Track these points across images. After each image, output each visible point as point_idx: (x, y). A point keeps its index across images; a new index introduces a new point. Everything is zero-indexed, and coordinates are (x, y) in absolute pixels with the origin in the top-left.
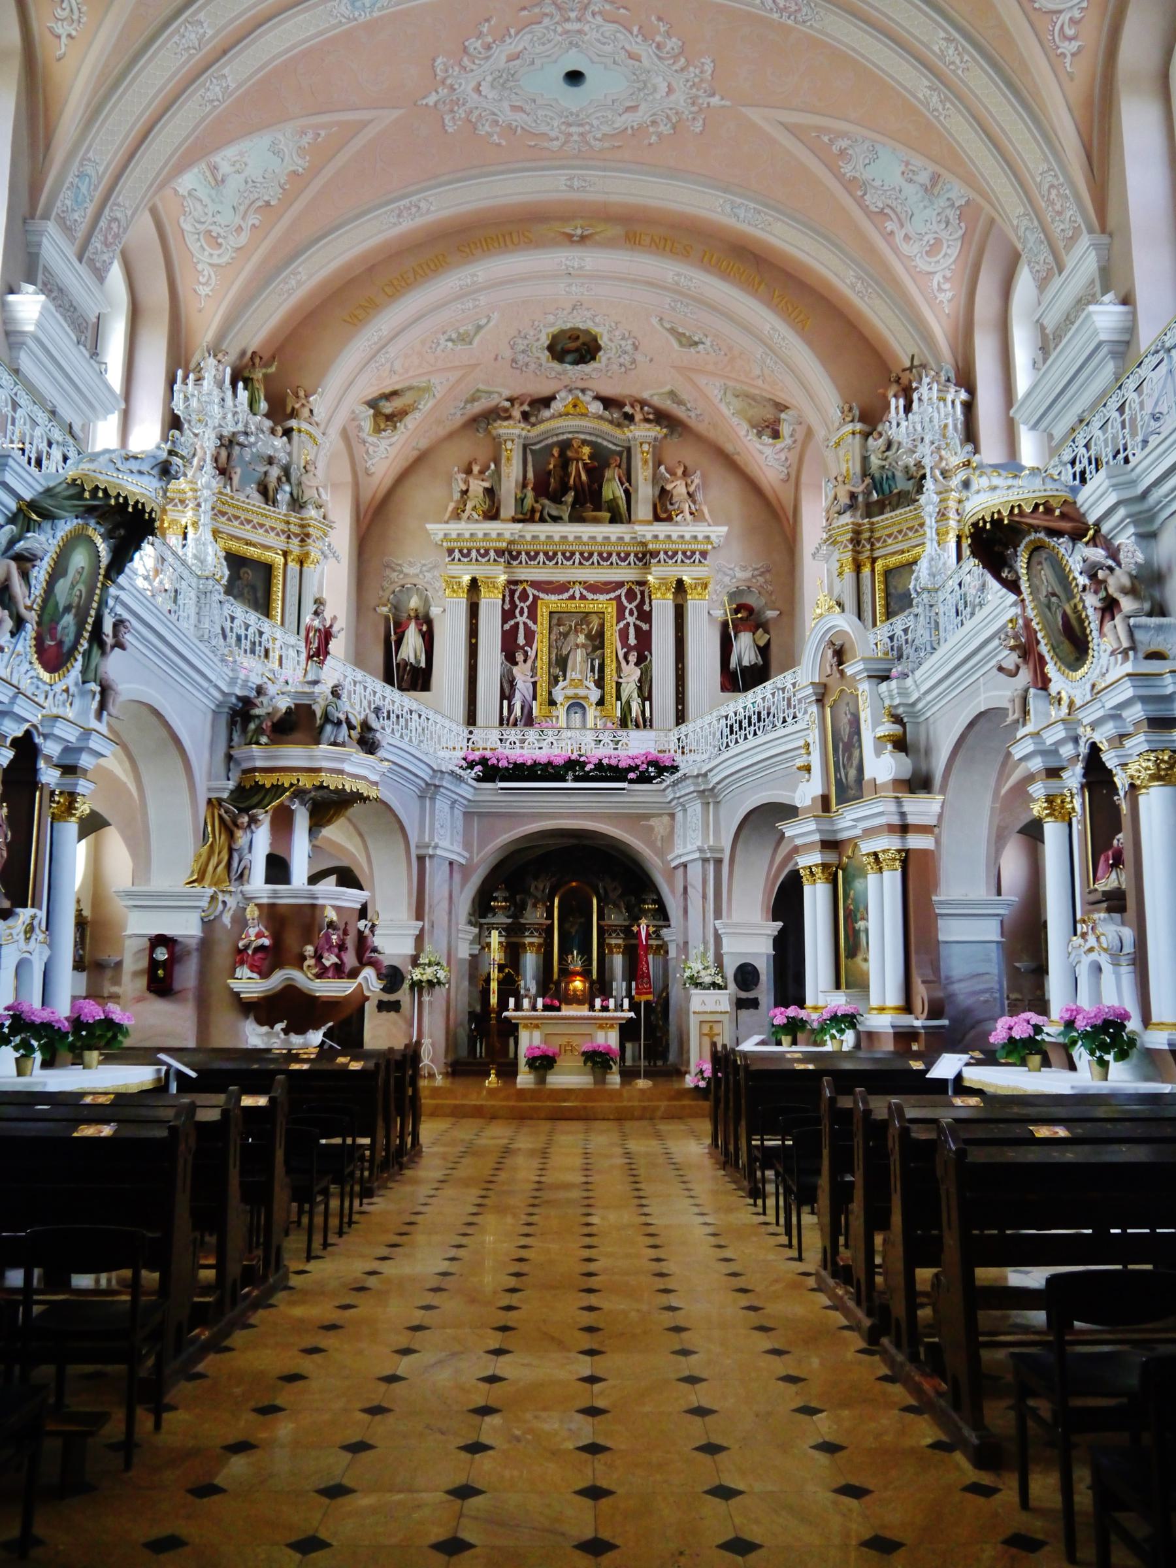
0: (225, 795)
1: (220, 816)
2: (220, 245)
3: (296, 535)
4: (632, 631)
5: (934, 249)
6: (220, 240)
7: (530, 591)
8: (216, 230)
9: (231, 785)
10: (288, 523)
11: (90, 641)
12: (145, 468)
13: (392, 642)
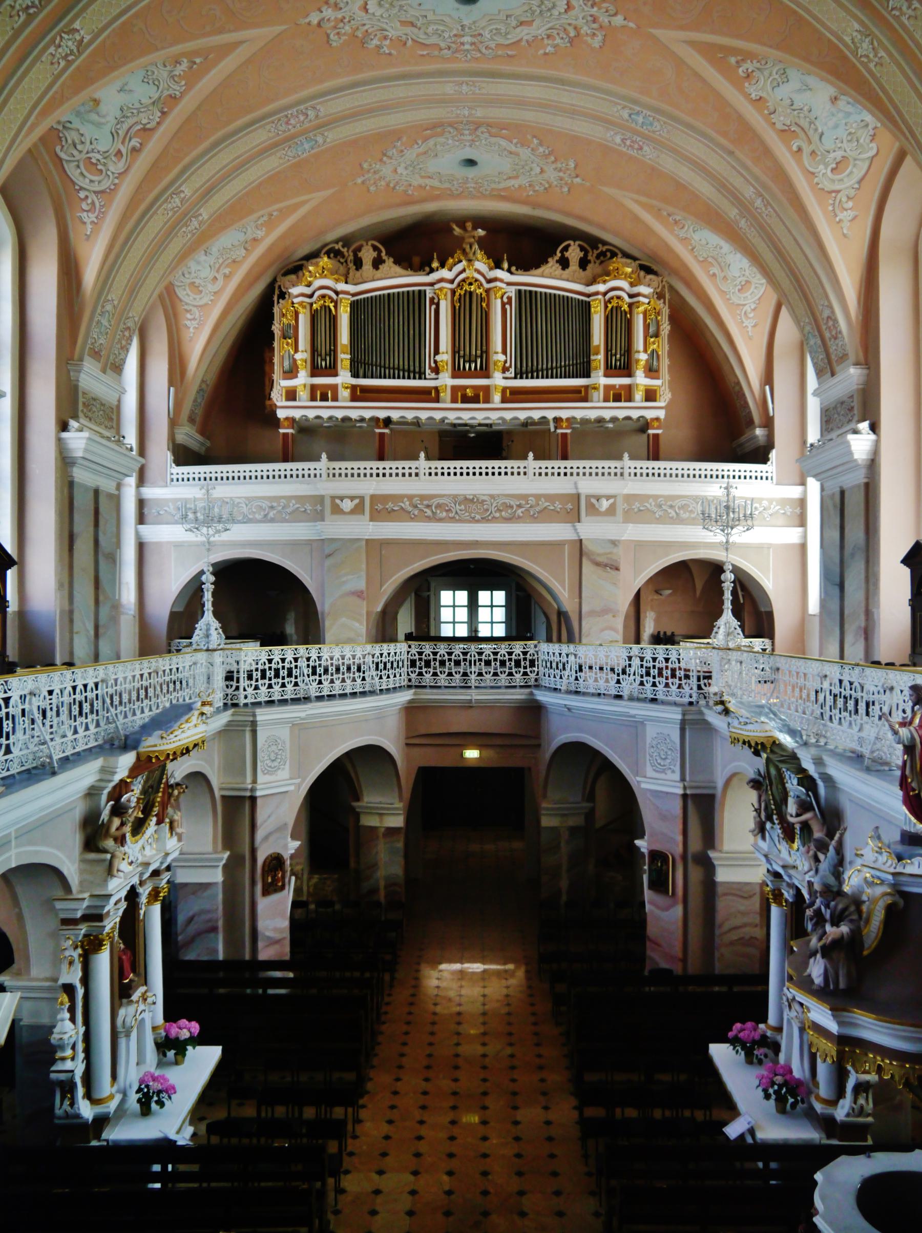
2: (201, 292)
5: (744, 287)
6: (201, 288)
8: (197, 281)
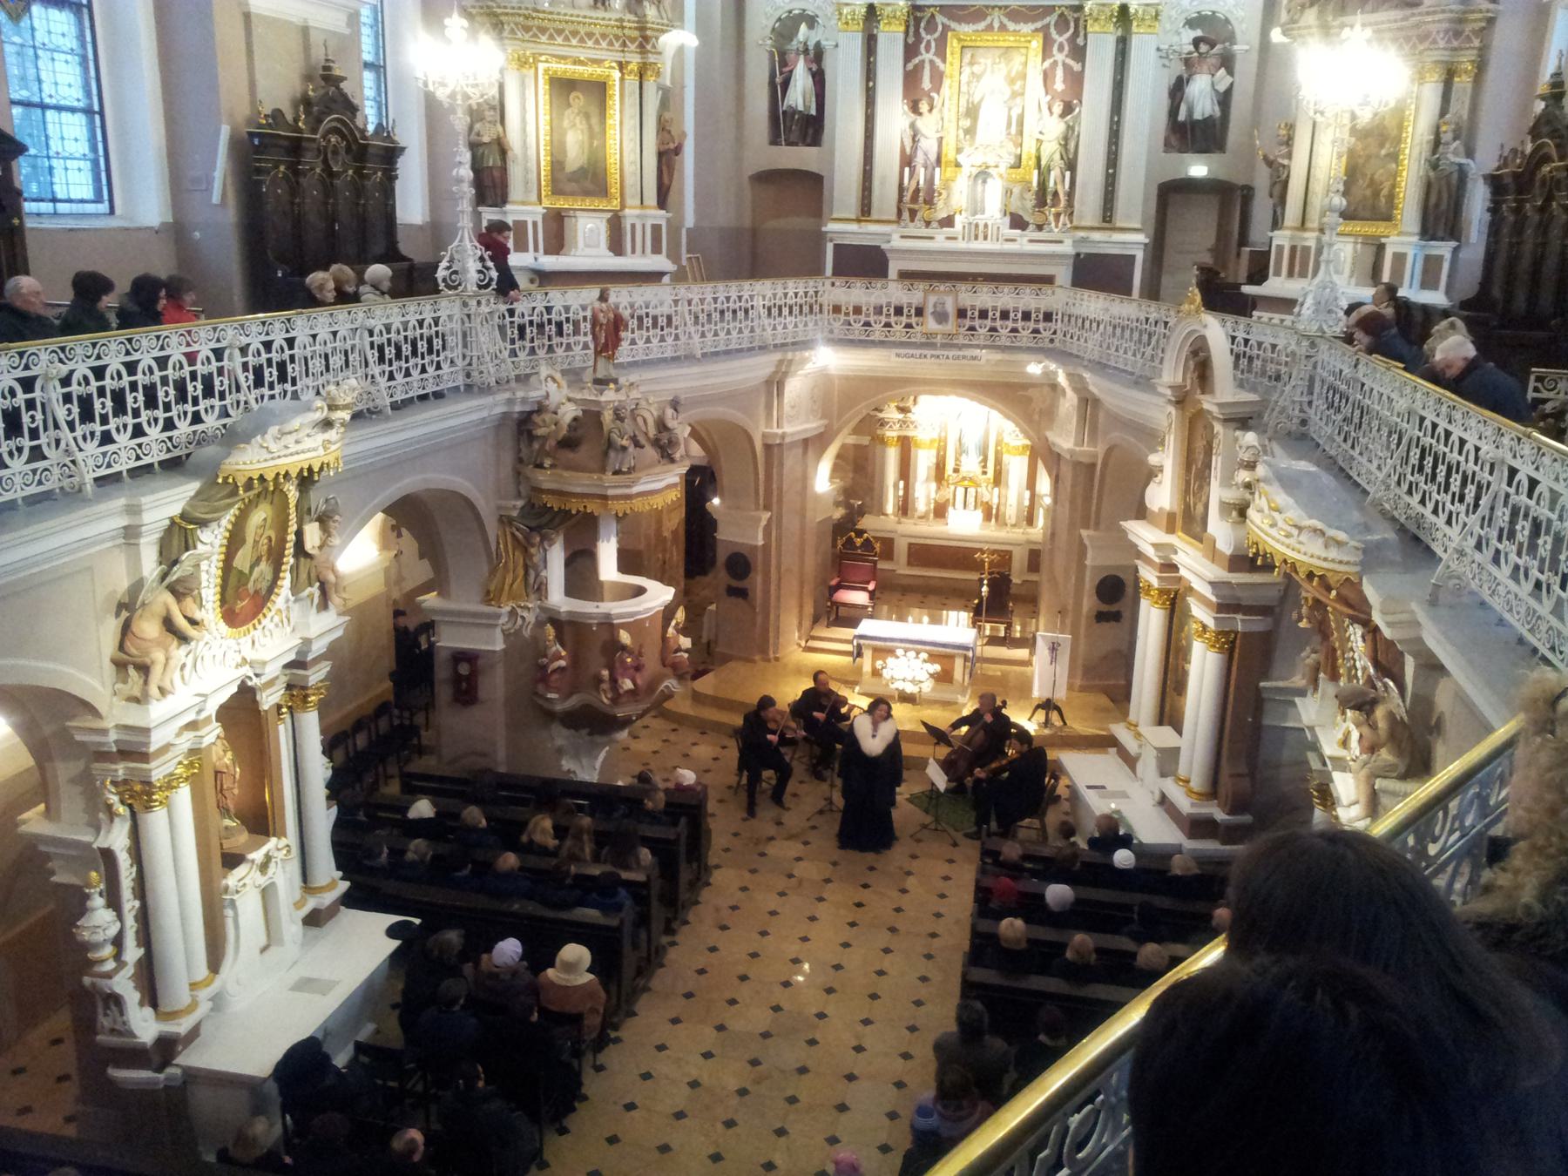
0: (515, 514)
1: (513, 535)
3: (633, 40)
4: (1060, 72)
7: (940, 19)
9: (520, 503)
10: (623, 28)
11: (296, 556)
12: (308, 431)
13: (779, 86)
